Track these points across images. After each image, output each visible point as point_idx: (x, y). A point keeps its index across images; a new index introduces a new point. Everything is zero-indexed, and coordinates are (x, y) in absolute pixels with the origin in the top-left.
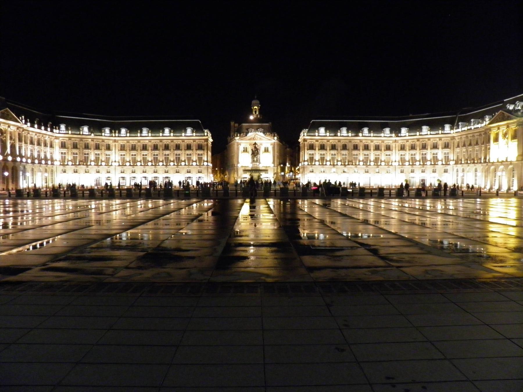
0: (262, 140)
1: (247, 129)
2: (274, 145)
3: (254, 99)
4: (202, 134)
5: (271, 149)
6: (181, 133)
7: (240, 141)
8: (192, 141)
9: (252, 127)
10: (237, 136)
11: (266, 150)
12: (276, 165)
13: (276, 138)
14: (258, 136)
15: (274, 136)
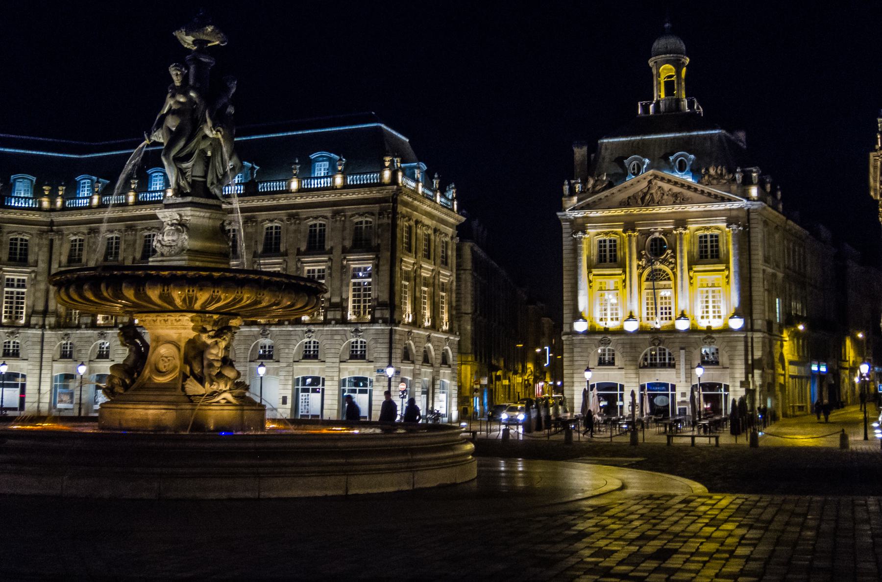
0: (684, 201)
1: (620, 161)
2: (743, 224)
3: (663, 33)
4: (373, 178)
5: (730, 248)
6: (288, 180)
7: (579, 214)
8: (327, 212)
9: (642, 149)
10: (572, 193)
11: (708, 253)
12: (759, 323)
13: (754, 192)
14: (666, 186)
15: (747, 181)
